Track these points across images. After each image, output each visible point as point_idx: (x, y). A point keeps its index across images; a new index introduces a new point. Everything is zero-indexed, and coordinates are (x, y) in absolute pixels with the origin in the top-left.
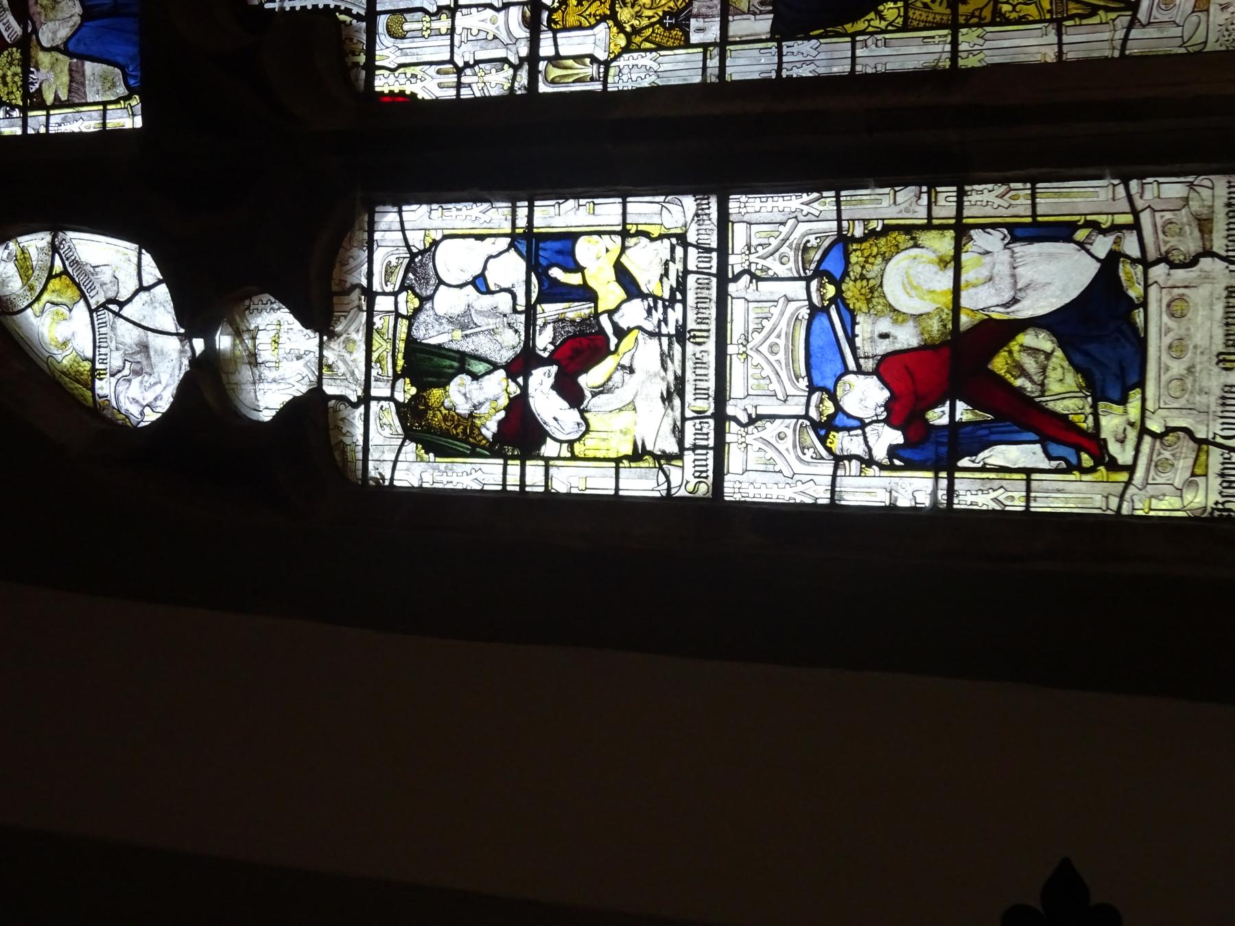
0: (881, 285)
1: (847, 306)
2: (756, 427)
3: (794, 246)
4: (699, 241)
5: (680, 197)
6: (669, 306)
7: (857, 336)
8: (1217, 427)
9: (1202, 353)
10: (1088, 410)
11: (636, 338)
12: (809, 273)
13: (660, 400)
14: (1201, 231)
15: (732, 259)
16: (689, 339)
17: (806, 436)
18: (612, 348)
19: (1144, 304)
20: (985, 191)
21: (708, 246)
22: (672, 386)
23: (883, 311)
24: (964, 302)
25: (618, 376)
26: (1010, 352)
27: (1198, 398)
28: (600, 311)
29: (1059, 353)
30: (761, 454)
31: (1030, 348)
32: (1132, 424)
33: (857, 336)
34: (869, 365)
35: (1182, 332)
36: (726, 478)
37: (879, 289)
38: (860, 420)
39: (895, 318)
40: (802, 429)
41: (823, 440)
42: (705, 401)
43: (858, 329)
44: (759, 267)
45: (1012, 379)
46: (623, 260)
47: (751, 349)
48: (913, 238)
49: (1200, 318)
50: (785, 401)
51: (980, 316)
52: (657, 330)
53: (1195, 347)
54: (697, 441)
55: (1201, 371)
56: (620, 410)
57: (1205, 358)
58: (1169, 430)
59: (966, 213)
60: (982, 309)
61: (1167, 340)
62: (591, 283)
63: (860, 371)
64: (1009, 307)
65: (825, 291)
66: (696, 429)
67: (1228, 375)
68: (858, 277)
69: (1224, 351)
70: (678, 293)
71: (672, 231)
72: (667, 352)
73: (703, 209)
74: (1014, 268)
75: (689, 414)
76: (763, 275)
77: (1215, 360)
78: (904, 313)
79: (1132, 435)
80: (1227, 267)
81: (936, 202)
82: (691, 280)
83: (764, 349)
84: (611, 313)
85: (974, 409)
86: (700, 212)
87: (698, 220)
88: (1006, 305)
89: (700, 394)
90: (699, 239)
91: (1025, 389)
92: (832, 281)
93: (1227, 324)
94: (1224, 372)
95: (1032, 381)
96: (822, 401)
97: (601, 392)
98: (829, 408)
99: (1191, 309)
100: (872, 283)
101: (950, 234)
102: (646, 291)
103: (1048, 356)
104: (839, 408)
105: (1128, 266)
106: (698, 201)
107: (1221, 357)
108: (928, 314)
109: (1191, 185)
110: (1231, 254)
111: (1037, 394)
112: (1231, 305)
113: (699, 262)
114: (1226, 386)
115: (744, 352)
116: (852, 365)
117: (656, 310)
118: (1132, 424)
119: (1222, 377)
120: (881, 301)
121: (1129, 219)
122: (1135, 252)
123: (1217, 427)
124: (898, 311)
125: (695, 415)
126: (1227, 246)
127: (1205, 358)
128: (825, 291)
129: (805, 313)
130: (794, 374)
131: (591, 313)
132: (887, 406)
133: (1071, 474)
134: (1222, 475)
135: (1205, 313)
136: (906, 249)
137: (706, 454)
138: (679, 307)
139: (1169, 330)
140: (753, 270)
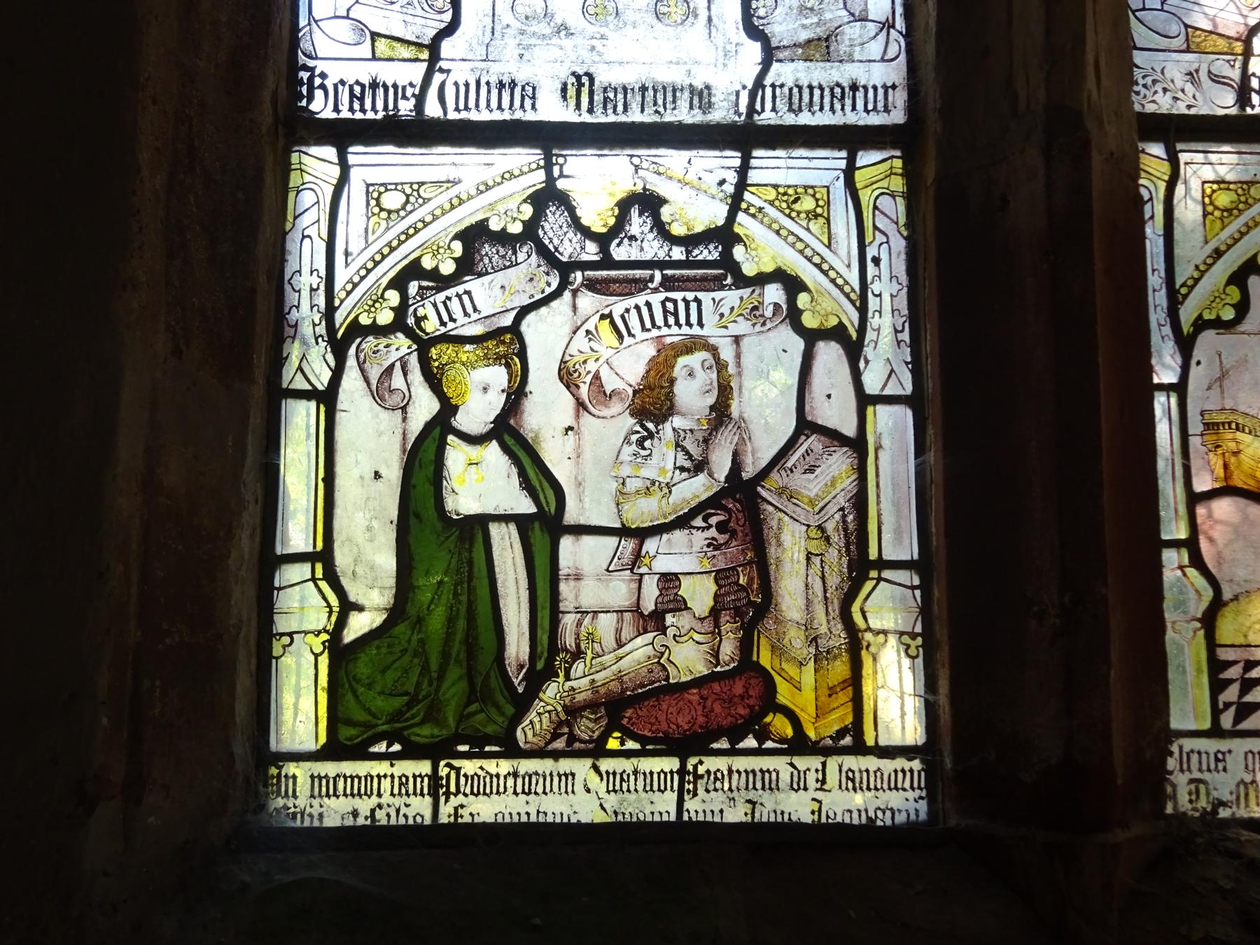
8: (462, 74)
14: (809, 41)
35: (629, 16)
57: (586, 54)
69: (597, 83)
80: (744, 87)
93: (644, 89)
94: (560, 86)
107: (585, 80)
109: (888, 25)
110: (769, 91)
112: (678, 94)
114: (534, 88)
126: (782, 86)
127: (586, 54)
134: (374, 85)
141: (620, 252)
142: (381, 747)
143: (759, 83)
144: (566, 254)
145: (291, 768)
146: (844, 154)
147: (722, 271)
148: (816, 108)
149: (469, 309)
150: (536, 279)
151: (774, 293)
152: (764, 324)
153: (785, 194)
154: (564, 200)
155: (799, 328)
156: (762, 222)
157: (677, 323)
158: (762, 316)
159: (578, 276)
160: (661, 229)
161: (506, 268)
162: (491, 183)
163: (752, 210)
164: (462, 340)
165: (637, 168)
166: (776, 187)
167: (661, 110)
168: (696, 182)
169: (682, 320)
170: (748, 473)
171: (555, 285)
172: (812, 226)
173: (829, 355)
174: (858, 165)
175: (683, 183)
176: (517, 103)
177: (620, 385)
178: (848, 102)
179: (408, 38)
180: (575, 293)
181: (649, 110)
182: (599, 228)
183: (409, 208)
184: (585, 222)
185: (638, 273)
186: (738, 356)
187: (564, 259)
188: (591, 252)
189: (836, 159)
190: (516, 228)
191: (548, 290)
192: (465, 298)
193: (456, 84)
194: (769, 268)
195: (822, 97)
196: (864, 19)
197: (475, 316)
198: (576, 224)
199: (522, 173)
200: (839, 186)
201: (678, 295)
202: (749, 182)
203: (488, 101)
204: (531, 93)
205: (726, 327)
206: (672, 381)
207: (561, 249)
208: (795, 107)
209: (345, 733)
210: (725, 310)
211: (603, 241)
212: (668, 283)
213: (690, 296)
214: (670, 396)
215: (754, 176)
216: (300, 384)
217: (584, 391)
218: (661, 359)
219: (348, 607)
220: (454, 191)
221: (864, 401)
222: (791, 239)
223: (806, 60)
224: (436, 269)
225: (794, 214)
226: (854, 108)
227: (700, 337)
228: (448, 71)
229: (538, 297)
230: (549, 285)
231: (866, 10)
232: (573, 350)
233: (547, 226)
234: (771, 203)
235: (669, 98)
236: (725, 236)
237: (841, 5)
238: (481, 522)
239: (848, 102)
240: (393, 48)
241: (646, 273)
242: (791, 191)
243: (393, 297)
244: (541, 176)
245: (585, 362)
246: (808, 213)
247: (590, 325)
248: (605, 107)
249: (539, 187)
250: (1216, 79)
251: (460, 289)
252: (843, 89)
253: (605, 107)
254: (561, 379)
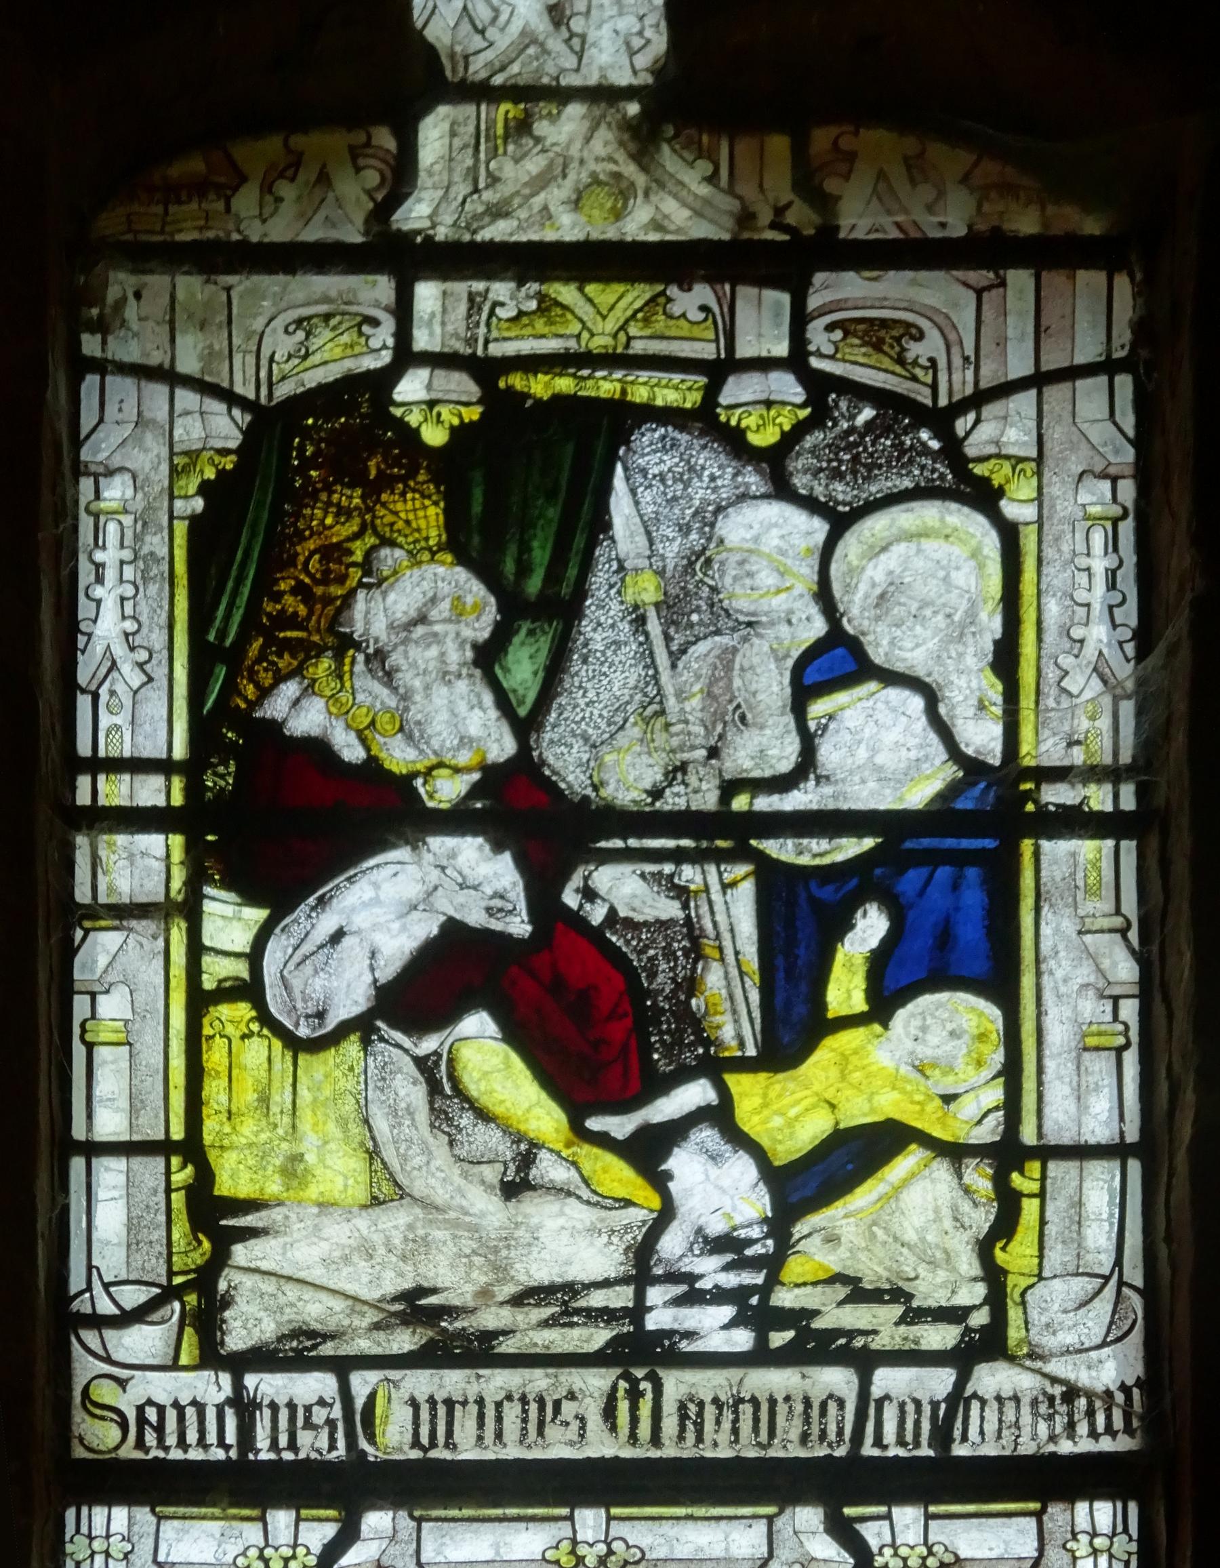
4: (975, 1406)
5: (1137, 1336)
11: (628, 1203)
13: (408, 1284)
15: (908, 1517)
16: (626, 1376)
18: (595, 1124)
21: (957, 1434)
22: (458, 1325)
25: (487, 1139)
28: (731, 1080)
36: (143, 1514)
42: (408, 1437)
52: (658, 1271)
54: (267, 1413)
56: (373, 1154)
66: (308, 1409)
70: (790, 1334)
71: (1014, 1314)
72: (582, 1303)
73: (1090, 1413)
75: (362, 1383)
86: (1082, 1403)
87: (1051, 1399)
89: (433, 1417)
90: (983, 1402)
97: (434, 1088)
102: (799, 1229)
106: (1120, 1398)
113: (902, 1406)
117: (727, 1268)
125: (359, 1403)
131: (719, 1044)
137: (222, 1443)
138: (742, 1340)
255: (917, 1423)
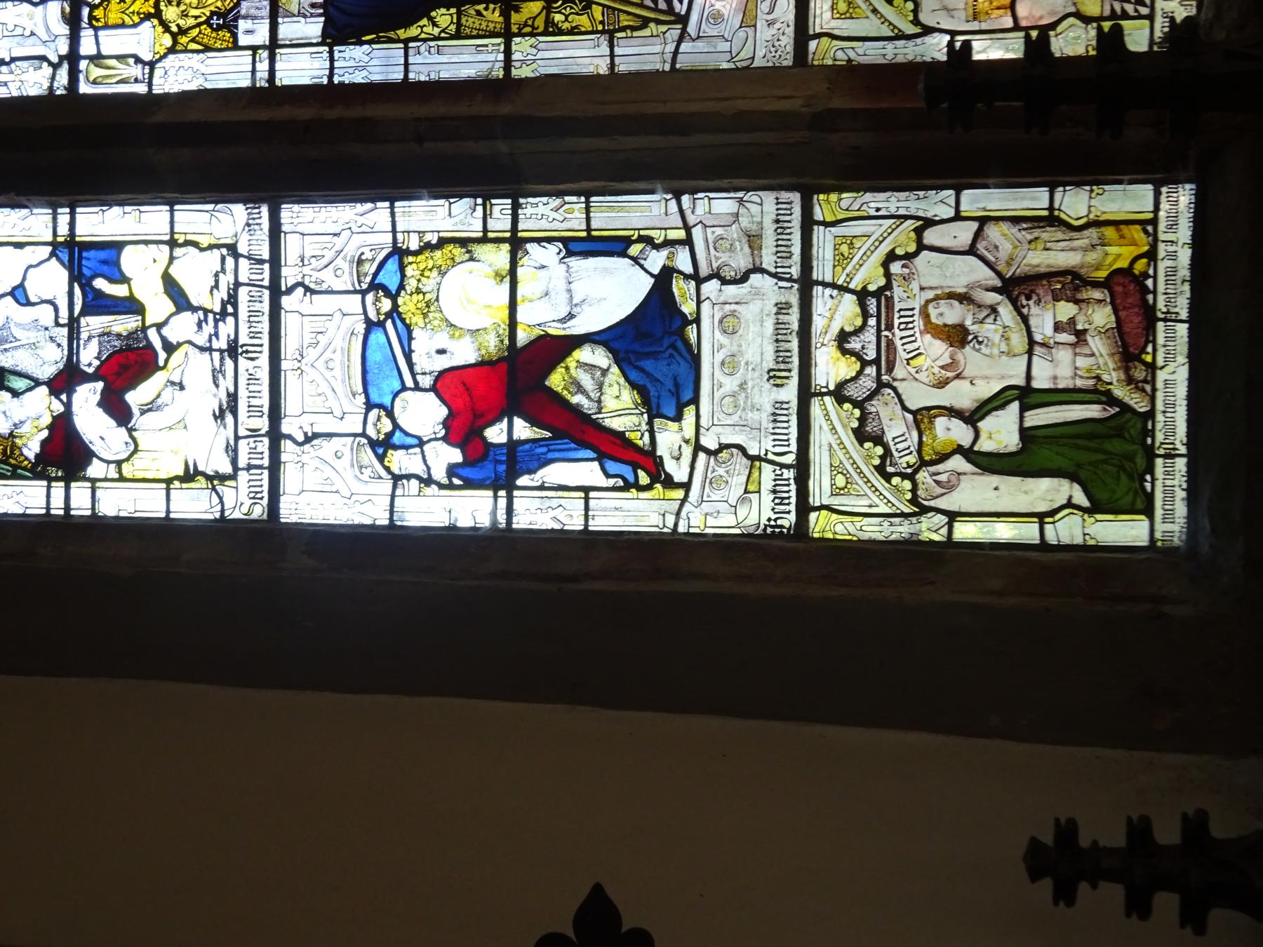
0: (437, 300)
1: (403, 321)
2: (312, 446)
3: (348, 259)
5: (230, 206)
6: (220, 320)
7: (413, 351)
8: (768, 444)
9: (753, 369)
10: (644, 427)
12: (365, 286)
13: (212, 418)
14: (750, 247)
16: (241, 354)
17: (363, 455)
18: (161, 363)
19: (697, 321)
20: (540, 204)
23: (440, 326)
24: (521, 316)
26: (567, 368)
27: (750, 415)
28: (147, 324)
29: (615, 369)
30: (319, 472)
31: (586, 364)
32: (687, 442)
33: (413, 351)
34: (426, 381)
35: (735, 348)
37: (436, 304)
38: (419, 438)
39: (452, 333)
40: (360, 448)
41: (381, 458)
43: (414, 345)
44: (313, 279)
45: (570, 395)
46: (170, 271)
47: (306, 365)
48: (469, 252)
49: (750, 334)
50: (342, 419)
51: (537, 332)
53: (747, 364)
54: (251, 461)
55: (753, 387)
57: (756, 374)
58: (723, 447)
59: (521, 226)
60: (538, 325)
61: (719, 357)
62: (137, 295)
63: (417, 388)
64: (565, 323)
65: (380, 305)
67: (778, 393)
68: (414, 290)
69: (774, 367)
73: (254, 219)
74: (570, 283)
75: (242, 432)
76: (317, 288)
77: (767, 376)
78: (461, 329)
79: (687, 451)
80: (776, 284)
81: (491, 214)
82: (243, 293)
83: (320, 364)
84: (159, 326)
85: (532, 426)
88: (562, 321)
91: (582, 406)
92: (388, 293)
94: (775, 388)
95: (588, 397)
96: (379, 419)
97: (150, 410)
98: (387, 426)
99: (742, 326)
100: (428, 297)
101: (506, 247)
103: (605, 372)
104: (396, 426)
105: (681, 282)
106: (249, 210)
107: (772, 374)
108: (485, 329)
109: (741, 201)
110: (779, 270)
111: (593, 411)
112: (780, 321)
114: (777, 402)
115: (299, 368)
116: (409, 383)
117: (207, 324)
118: (687, 442)
119: (773, 394)
120: (438, 315)
121: (681, 234)
122: (689, 269)
123: (768, 444)
124: (455, 326)
125: (249, 433)
126: (776, 262)
127: (756, 374)
128: (380, 305)
129: (361, 328)
130: (351, 390)
131: (138, 327)
132: (446, 423)
133: (628, 491)
135: (756, 329)
136: (462, 262)
138: (230, 320)
139: (721, 346)
140: (307, 283)
141: (871, 354)
142: (1148, 486)
143: (774, 275)
144: (872, 384)
145: (1158, 535)
146: (815, 227)
147: (883, 297)
148: (789, 243)
149: (903, 438)
150: (886, 401)
151: (896, 268)
152: (913, 274)
153: (838, 261)
154: (841, 385)
155: (915, 254)
156: (855, 274)
157: (912, 322)
158: (909, 274)
159: (885, 378)
160: (858, 331)
161: (879, 418)
162: (831, 427)
163: (848, 280)
164: (920, 443)
165: (823, 345)
166: (834, 266)
167: (789, 331)
168: (832, 311)
169: (911, 319)
170: (998, 283)
171: (890, 391)
172: (857, 246)
173: (931, 237)
174: (822, 219)
175: (831, 319)
176: (785, 412)
177: (947, 354)
178: (786, 225)
179: (747, 473)
180: (894, 380)
181: (789, 338)
182: (858, 366)
183: (845, 472)
184: (854, 374)
185: (883, 344)
186: (931, 288)
187: (875, 385)
188: (871, 371)
189: (818, 232)
190: (857, 412)
191: (893, 394)
192: (896, 440)
193: (774, 446)
194: (881, 270)
195: (783, 240)
196: (737, 215)
197: (907, 435)
198: (854, 379)
199: (826, 409)
200: (832, 229)
201: (896, 322)
202: (831, 281)
203: (784, 428)
204: (779, 404)
205: (915, 295)
206: (945, 325)
207: (869, 387)
208: (788, 255)
209: (1139, 504)
210: (905, 295)
211: (864, 364)
212: (890, 327)
213: (897, 315)
214: (954, 326)
215: (828, 279)
216: (944, 531)
217: (950, 374)
218: (933, 331)
219: (1069, 504)
220: (835, 446)
221: (958, 217)
222: (864, 258)
223: (761, 249)
224: (880, 457)
225: (851, 256)
226: (789, 222)
227: (920, 309)
228: (767, 451)
229: (896, 400)
230: (889, 394)
231: (732, 214)
232: (926, 381)
233: (856, 395)
234: (844, 269)
235: (783, 326)
236: (862, 295)
237: (729, 228)
238: (1024, 432)
239: (786, 225)
240: (753, 482)
241: (883, 340)
242: (837, 258)
243: (896, 480)
244: (827, 399)
245: (934, 374)
246: (850, 249)
247: (913, 371)
248: (788, 363)
249: (833, 400)
250: (771, 12)
251: (891, 443)
252: (778, 228)
253: (788, 363)
254: (943, 387)
255: (256, 269)
